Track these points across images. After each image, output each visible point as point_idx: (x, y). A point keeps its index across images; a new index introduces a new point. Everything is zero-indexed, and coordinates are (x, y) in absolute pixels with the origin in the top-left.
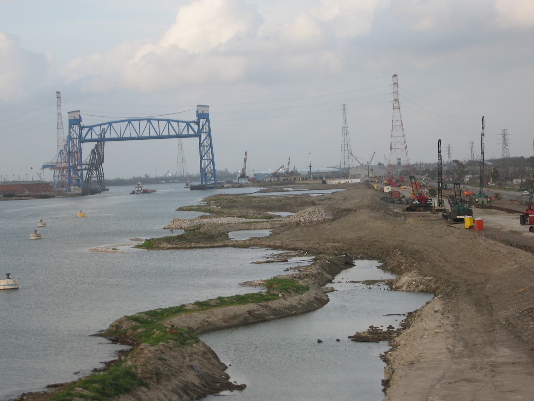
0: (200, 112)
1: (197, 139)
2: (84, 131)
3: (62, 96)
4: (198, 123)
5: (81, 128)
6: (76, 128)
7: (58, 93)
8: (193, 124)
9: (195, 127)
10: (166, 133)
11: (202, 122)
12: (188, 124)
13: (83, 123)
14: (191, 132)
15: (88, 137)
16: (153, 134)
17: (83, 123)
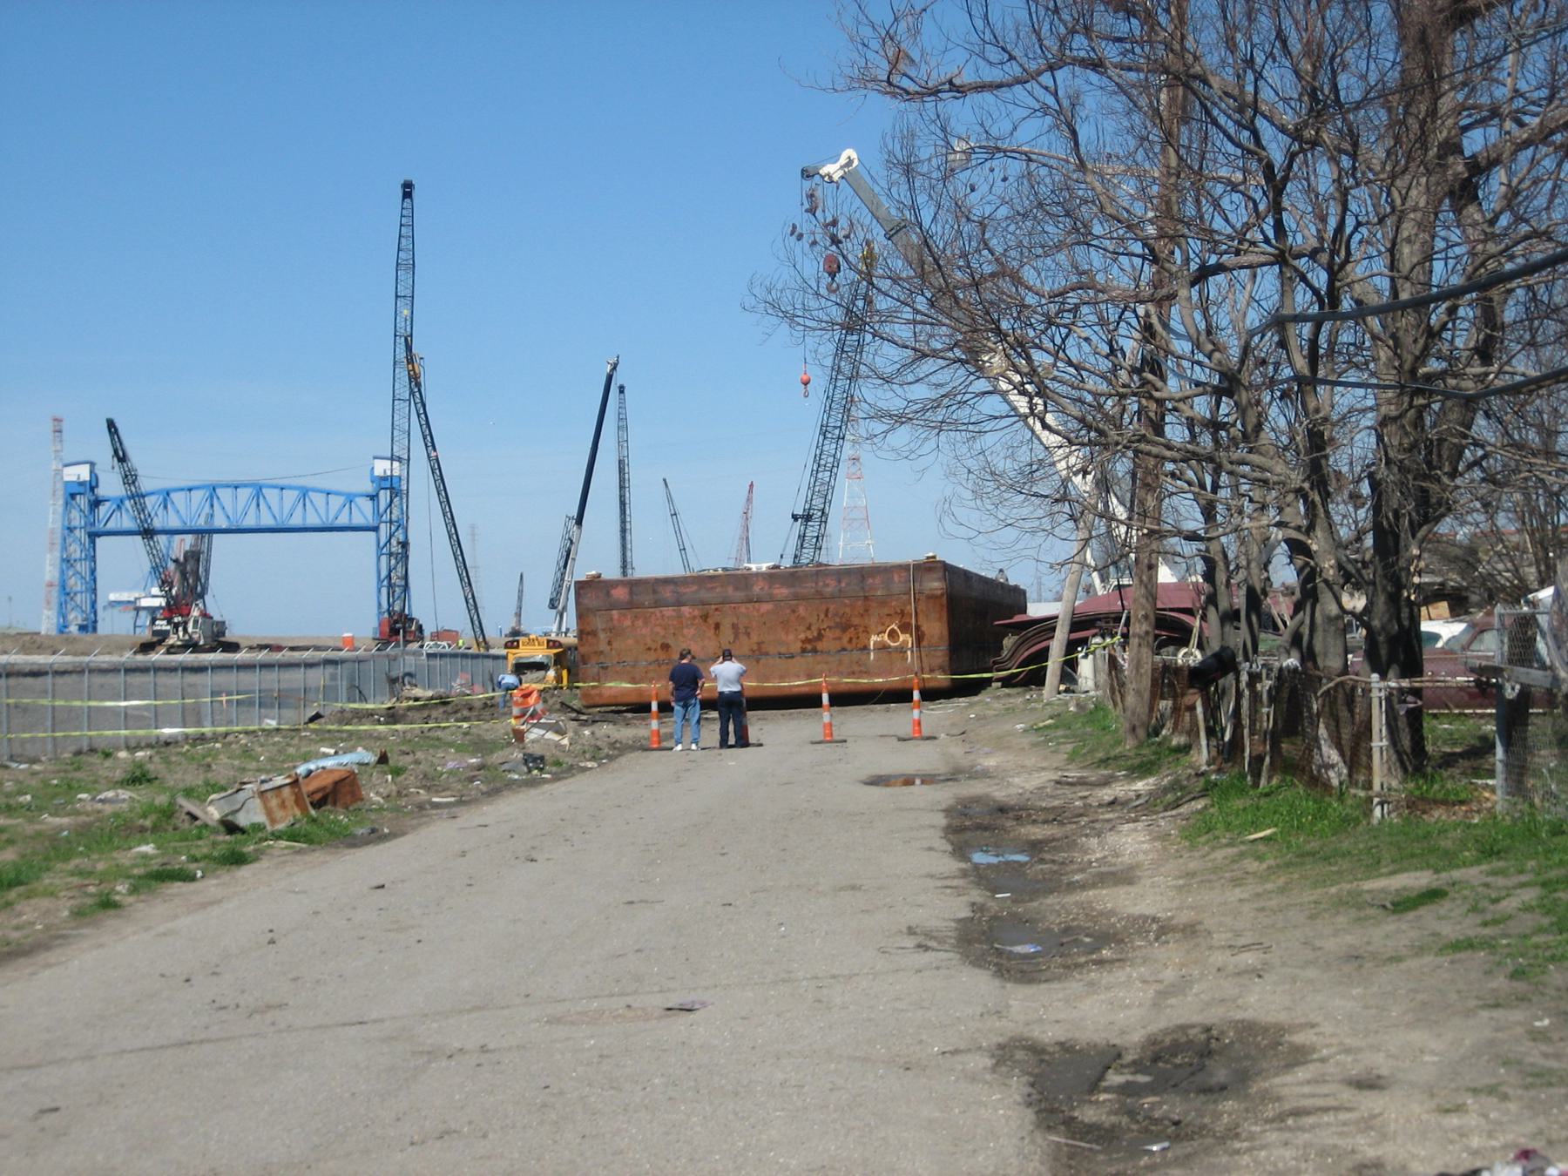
0: (378, 472)
1: (372, 534)
2: (103, 510)
3: (65, 426)
4: (373, 497)
5: (96, 503)
6: (82, 501)
7: (58, 420)
8: (364, 499)
9: (367, 505)
10: (296, 521)
11: (384, 497)
12: (350, 499)
13: (102, 491)
14: (358, 520)
15: (111, 525)
16: (267, 521)
17: (102, 491)
